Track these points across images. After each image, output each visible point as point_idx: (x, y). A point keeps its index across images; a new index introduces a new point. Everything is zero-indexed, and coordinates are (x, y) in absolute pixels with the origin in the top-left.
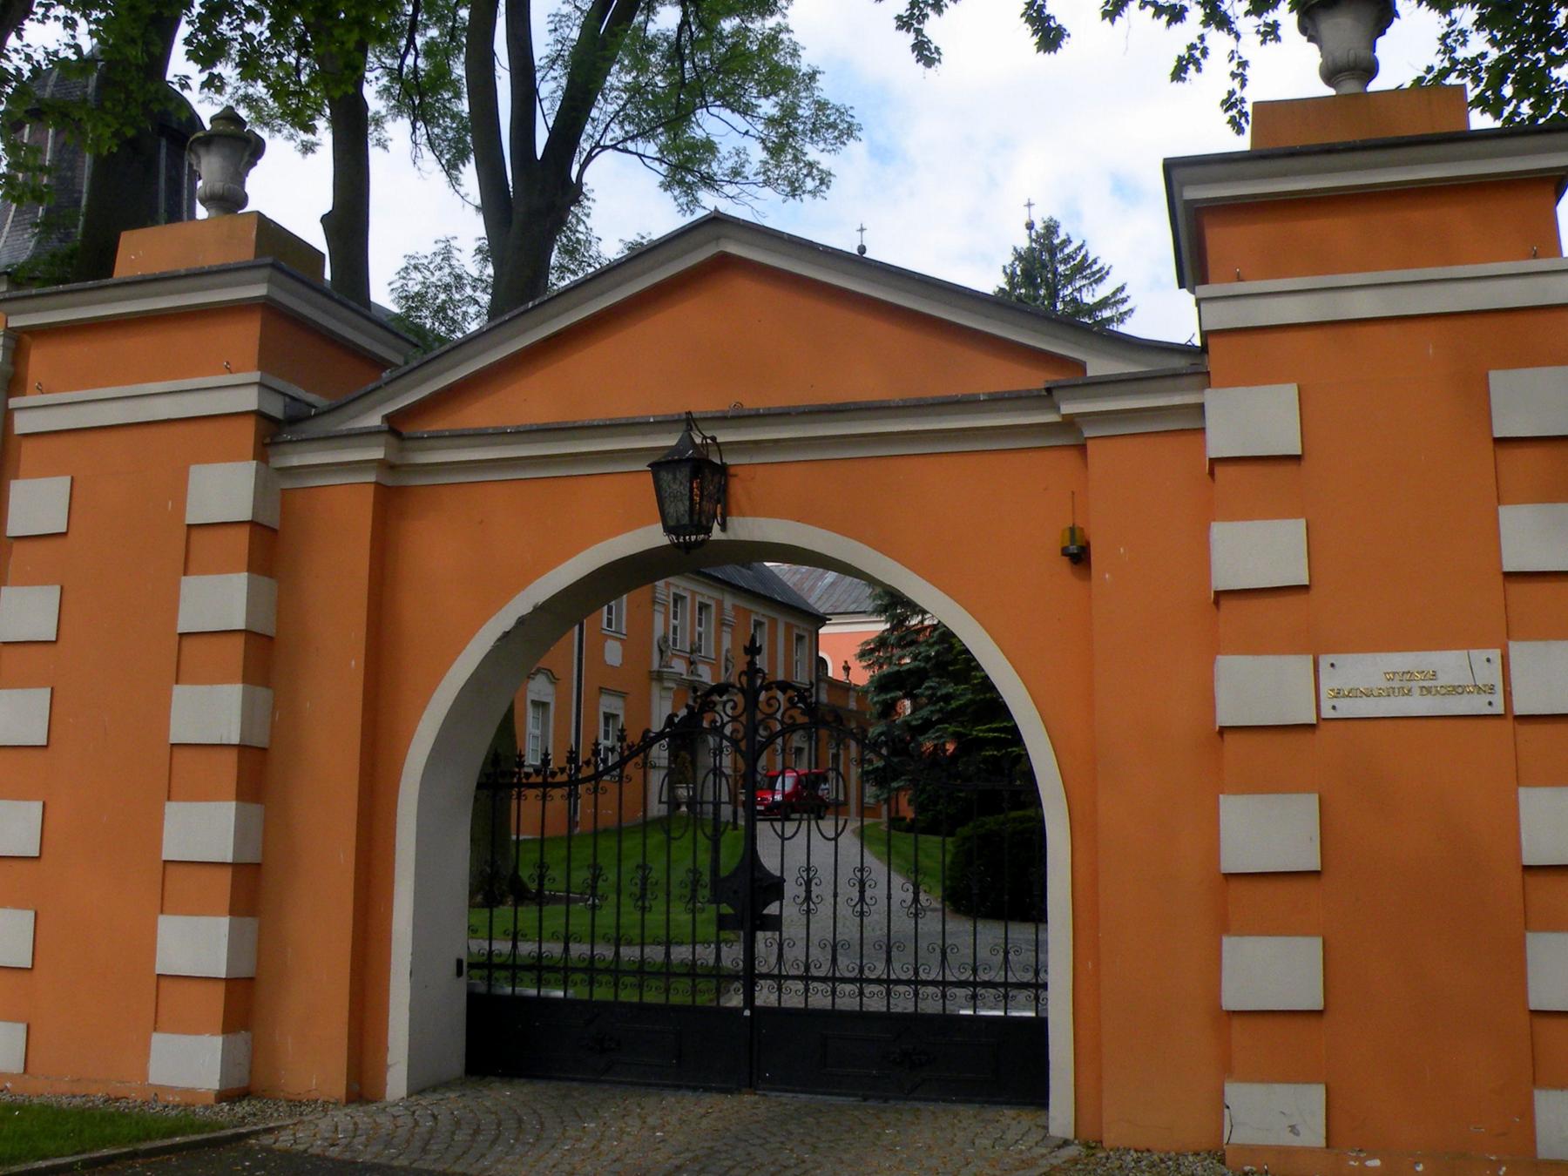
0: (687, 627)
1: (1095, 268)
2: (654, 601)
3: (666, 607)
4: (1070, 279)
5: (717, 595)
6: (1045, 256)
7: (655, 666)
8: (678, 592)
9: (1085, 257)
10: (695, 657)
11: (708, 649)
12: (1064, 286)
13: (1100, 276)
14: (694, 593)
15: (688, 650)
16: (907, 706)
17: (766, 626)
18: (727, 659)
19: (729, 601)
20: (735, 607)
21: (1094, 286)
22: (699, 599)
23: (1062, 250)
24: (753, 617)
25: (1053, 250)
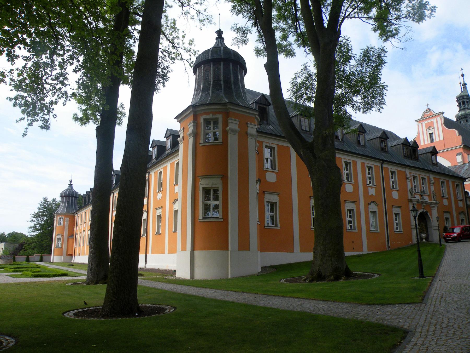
0: (419, 185)
2: (406, 179)
3: (411, 180)
5: (427, 175)
7: (410, 198)
10: (423, 194)
11: (427, 191)
15: (420, 192)
17: (445, 183)
18: (433, 194)
19: (431, 176)
20: (433, 178)
22: (421, 176)
24: (440, 180)
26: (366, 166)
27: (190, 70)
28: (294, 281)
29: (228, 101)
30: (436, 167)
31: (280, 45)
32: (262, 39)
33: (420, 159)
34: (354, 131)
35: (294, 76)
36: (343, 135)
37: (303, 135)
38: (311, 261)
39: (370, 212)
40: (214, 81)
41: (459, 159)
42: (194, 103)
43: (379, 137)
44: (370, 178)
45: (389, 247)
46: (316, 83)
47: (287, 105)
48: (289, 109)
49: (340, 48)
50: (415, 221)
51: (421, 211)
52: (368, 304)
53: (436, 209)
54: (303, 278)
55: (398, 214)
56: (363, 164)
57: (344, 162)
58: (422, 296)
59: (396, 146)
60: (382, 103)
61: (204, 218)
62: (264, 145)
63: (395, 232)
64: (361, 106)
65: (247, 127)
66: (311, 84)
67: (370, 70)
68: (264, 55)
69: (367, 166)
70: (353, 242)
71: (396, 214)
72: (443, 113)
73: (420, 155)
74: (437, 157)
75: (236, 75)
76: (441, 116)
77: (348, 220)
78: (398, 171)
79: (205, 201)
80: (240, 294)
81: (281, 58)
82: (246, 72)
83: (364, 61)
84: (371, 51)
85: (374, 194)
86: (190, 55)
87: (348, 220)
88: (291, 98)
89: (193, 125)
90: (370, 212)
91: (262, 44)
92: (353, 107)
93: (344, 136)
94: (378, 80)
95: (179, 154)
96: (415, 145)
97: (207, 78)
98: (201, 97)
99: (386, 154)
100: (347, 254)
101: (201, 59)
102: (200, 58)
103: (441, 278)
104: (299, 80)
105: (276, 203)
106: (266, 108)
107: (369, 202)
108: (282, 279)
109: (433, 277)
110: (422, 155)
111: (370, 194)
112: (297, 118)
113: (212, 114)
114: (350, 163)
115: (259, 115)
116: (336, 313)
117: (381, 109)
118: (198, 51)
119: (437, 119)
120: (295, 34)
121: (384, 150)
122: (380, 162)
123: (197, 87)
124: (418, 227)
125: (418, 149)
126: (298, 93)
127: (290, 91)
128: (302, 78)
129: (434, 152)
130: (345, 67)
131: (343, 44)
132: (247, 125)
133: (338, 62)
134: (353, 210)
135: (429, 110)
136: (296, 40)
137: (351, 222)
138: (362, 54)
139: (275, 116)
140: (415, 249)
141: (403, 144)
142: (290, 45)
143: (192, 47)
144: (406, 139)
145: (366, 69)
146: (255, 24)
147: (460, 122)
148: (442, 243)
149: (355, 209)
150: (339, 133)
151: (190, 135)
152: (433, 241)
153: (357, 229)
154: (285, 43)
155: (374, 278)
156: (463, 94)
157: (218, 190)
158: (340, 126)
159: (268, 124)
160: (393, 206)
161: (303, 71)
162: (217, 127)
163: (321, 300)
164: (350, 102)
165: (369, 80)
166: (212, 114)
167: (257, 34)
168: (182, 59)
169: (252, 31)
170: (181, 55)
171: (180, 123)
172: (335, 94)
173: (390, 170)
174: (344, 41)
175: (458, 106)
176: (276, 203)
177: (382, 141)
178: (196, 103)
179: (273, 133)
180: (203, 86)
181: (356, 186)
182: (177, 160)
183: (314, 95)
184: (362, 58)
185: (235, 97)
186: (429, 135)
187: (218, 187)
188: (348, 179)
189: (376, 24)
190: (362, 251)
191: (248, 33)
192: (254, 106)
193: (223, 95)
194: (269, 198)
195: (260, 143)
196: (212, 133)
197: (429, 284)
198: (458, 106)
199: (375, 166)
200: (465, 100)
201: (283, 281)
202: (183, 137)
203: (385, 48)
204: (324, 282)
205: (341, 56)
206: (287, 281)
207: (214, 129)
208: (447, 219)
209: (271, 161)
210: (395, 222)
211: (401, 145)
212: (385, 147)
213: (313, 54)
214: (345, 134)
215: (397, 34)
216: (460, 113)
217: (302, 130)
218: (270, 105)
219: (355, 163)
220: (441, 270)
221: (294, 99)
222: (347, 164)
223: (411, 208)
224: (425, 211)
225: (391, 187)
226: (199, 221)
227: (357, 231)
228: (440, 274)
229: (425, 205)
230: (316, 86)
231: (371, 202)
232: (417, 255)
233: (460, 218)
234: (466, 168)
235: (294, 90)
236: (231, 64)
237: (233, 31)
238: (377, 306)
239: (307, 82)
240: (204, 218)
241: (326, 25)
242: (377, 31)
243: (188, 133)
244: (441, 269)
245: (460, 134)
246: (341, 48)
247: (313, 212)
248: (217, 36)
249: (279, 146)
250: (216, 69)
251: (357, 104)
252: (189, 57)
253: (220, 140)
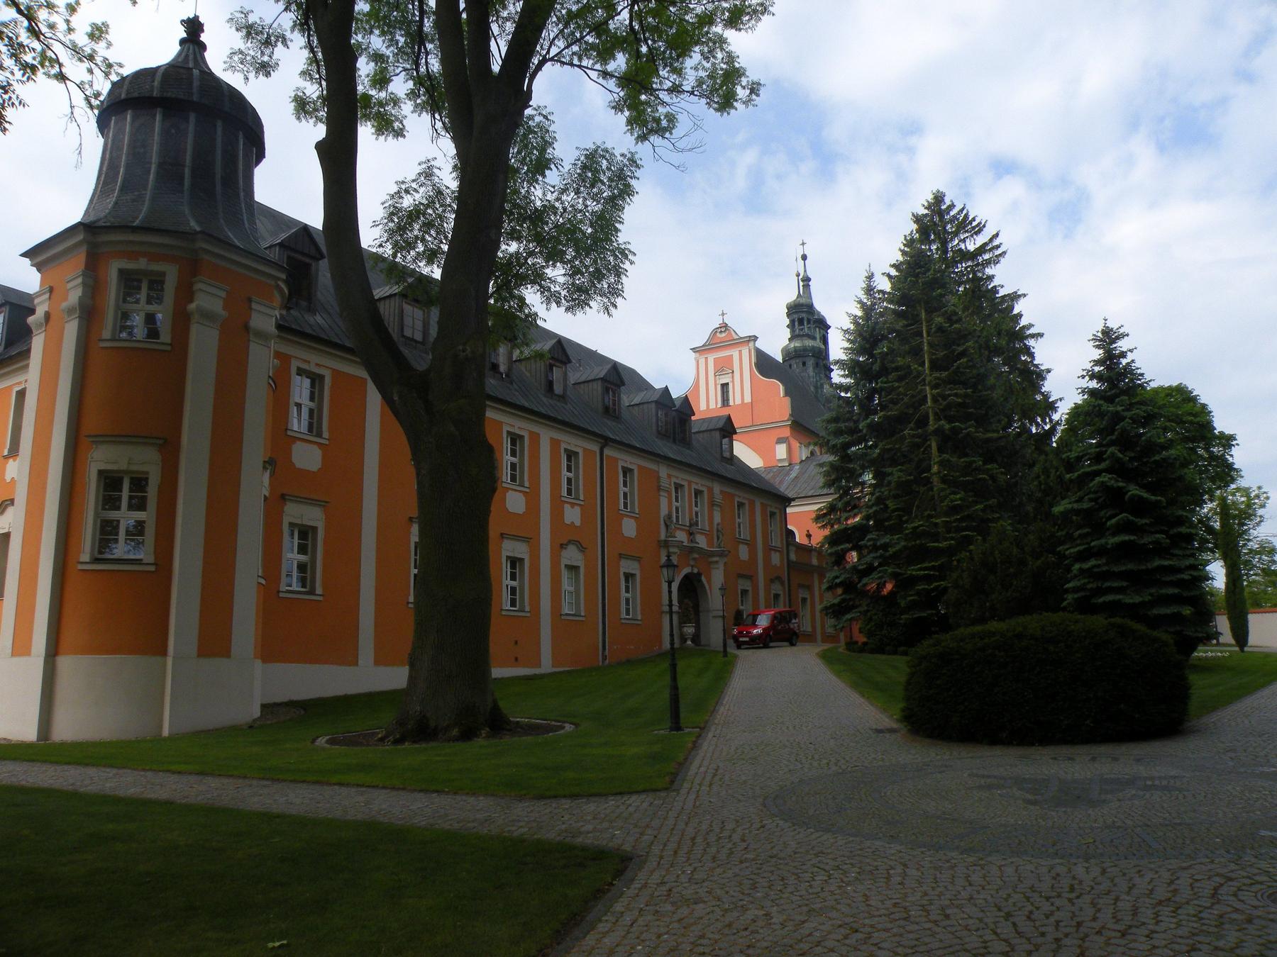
1: (974, 224)
2: (659, 489)
3: (669, 492)
4: (956, 234)
5: (709, 484)
6: (936, 219)
7: (663, 537)
8: (677, 481)
9: (966, 216)
10: (694, 529)
11: (703, 523)
12: (952, 240)
13: (979, 229)
14: (690, 483)
16: (853, 556)
17: (747, 506)
18: (718, 531)
19: (717, 488)
20: (721, 491)
21: (975, 236)
22: (694, 486)
23: (948, 213)
24: (737, 499)
25: (941, 214)
26: (562, 451)
27: (89, 120)
28: (351, 742)
29: (198, 229)
30: (728, 466)
31: (367, 97)
32: (318, 72)
33: (694, 443)
34: (539, 355)
35: (395, 189)
36: (511, 362)
37: (406, 352)
38: (402, 690)
39: (563, 566)
40: (160, 165)
41: (781, 451)
42: (92, 218)
43: (602, 378)
44: (569, 480)
45: (604, 658)
46: (453, 216)
47: (368, 265)
48: (373, 277)
49: (525, 136)
50: (670, 592)
51: (686, 570)
52: (541, 797)
53: (721, 566)
54: (378, 733)
55: (633, 575)
56: (555, 444)
57: (508, 432)
58: (671, 773)
59: (641, 407)
60: (615, 292)
61: (96, 560)
62: (294, 365)
63: (623, 621)
64: (564, 293)
65: (251, 309)
66: (440, 217)
67: (594, 207)
68: (319, 119)
69: (566, 450)
70: (516, 643)
71: (628, 576)
72: (755, 338)
73: (694, 433)
74: (734, 442)
75: (231, 160)
76: (751, 344)
77: (507, 586)
78: (640, 467)
79: (104, 509)
80: (192, 778)
81: (365, 132)
82: (260, 155)
83: (582, 177)
84: (604, 157)
85: (578, 523)
86: (90, 71)
87: (507, 586)
88: (381, 246)
89: (83, 283)
90: (563, 566)
91: (316, 86)
92: (542, 293)
93: (514, 366)
94: (612, 235)
95: (27, 366)
96: (684, 409)
97: (142, 150)
98: (116, 203)
99: (614, 424)
100: (497, 672)
101: (128, 92)
102: (125, 87)
103: (718, 732)
104: (407, 202)
105: (314, 529)
106: (311, 265)
107: (565, 542)
108: (318, 737)
109: (702, 729)
110: (701, 435)
111: (567, 521)
112: (395, 303)
113: (146, 260)
114: (522, 437)
115: (286, 282)
116: (458, 823)
117: (612, 309)
118: (121, 65)
119: (740, 351)
120: (412, 78)
121: (611, 412)
122: (599, 442)
123: (106, 173)
124: (675, 608)
125: (693, 418)
126: (401, 235)
127: (381, 226)
128: (417, 196)
129: (727, 429)
130: (532, 188)
131: (534, 127)
132: (251, 305)
133: (517, 171)
134: (521, 560)
135: (725, 327)
136: (412, 92)
137: (513, 590)
138: (579, 160)
139: (332, 290)
140: (665, 665)
141: (656, 402)
142: (396, 101)
143: (100, 48)
144: (666, 390)
145: (585, 199)
146: (303, 25)
147: (790, 366)
148: (728, 650)
149: (526, 557)
150: (502, 355)
151: (70, 311)
152: (709, 645)
153: (527, 609)
154: (383, 95)
155: (562, 732)
156: (801, 301)
157: (146, 479)
158: (506, 338)
159: (311, 310)
160: (621, 556)
161: (423, 178)
162: (159, 300)
163: (421, 791)
164: (537, 278)
165: (590, 230)
166: (146, 260)
167: (306, 53)
168: (61, 77)
169: (291, 41)
170: (61, 65)
171: (39, 270)
172: (500, 255)
173: (621, 464)
174: (538, 119)
175: (788, 326)
176: (314, 529)
177: (607, 390)
178: (98, 220)
179: (309, 331)
180: (126, 173)
181: (533, 498)
182: (20, 383)
183: (445, 248)
184: (578, 171)
185: (222, 221)
186: (719, 387)
187: (147, 473)
188: (513, 478)
189: (622, 94)
190: (539, 665)
191: (279, 44)
192: (274, 255)
193: (187, 211)
194: (295, 513)
195: (284, 359)
196: (142, 314)
197: (690, 745)
198: (788, 326)
199: (585, 450)
200: (804, 315)
201: (322, 741)
202: (48, 316)
203: (637, 156)
204: (433, 744)
205: (524, 158)
206: (332, 742)
207: (149, 302)
208: (744, 592)
209: (311, 411)
210: (624, 595)
211: (653, 406)
212: (614, 404)
213: (454, 139)
214: (516, 361)
215: (669, 129)
217: (403, 336)
218: (322, 257)
219: (535, 438)
220: (720, 712)
221: (388, 251)
222: (515, 439)
223: (664, 559)
224: (696, 571)
225: (622, 507)
226: (80, 567)
227: (528, 615)
228: (716, 721)
229: (696, 556)
230: (453, 224)
231: (570, 542)
232: (667, 679)
233: (773, 592)
234: (793, 475)
235: (391, 225)
236: (219, 123)
237: (234, 28)
238: (563, 801)
239: (430, 211)
240: (96, 560)
241: (496, 68)
242: (622, 111)
243: (64, 305)
244: (722, 709)
245: (787, 394)
246: (529, 135)
247: (416, 560)
248: (185, 35)
249: (336, 373)
250: (173, 131)
251: (552, 286)
252: (87, 77)
253: (166, 337)
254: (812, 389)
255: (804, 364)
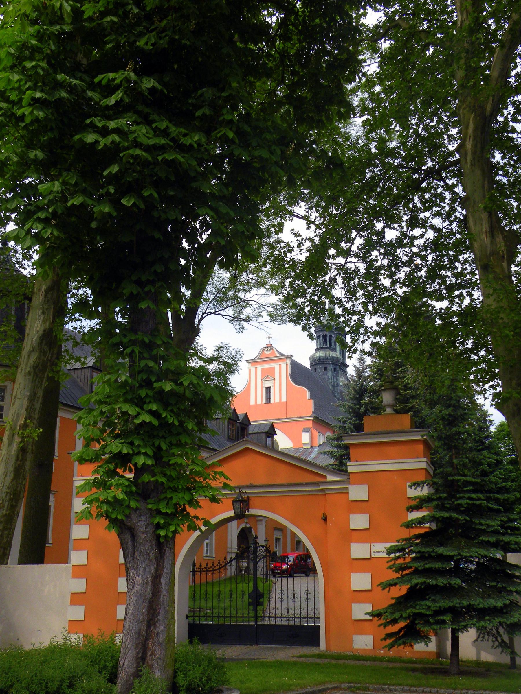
147: (316, 370)
186: (264, 390)
208: (278, 540)
216: (318, 355)
254: (331, 387)
255: (325, 369)
